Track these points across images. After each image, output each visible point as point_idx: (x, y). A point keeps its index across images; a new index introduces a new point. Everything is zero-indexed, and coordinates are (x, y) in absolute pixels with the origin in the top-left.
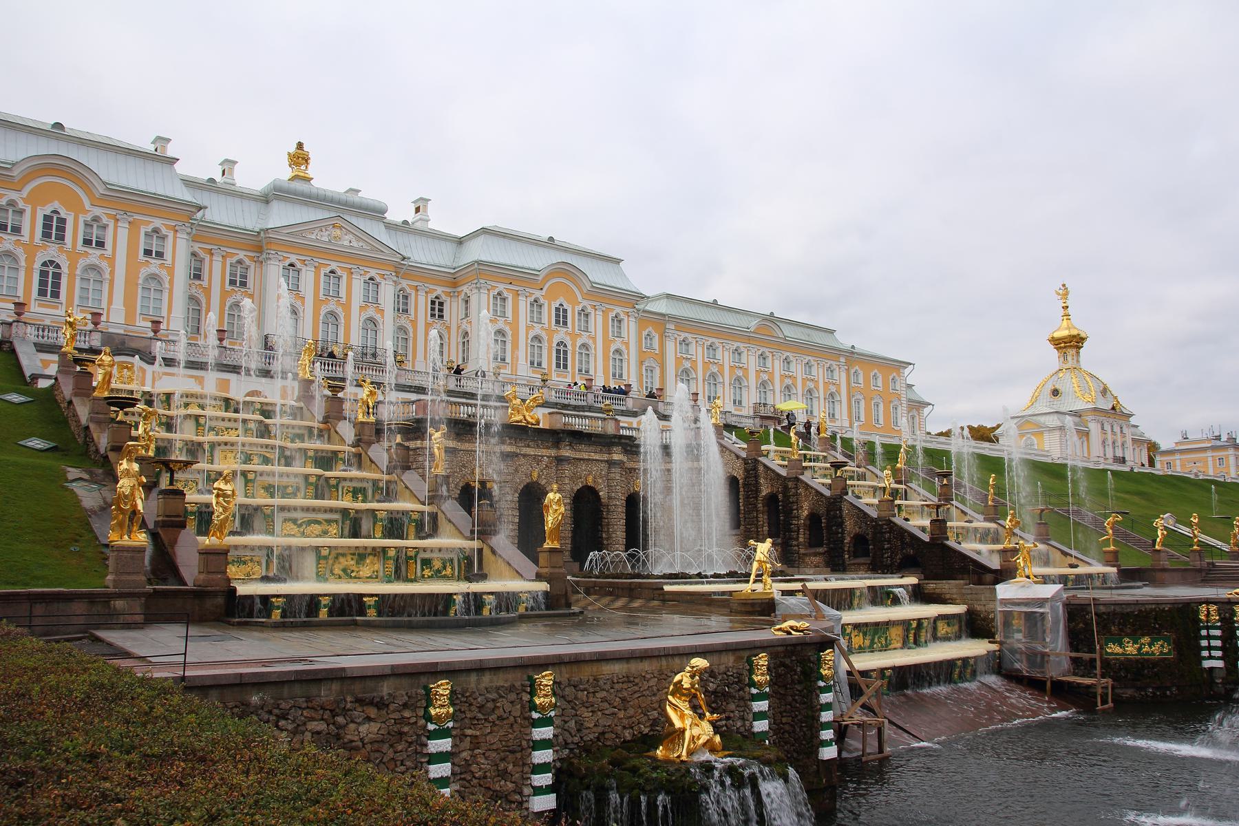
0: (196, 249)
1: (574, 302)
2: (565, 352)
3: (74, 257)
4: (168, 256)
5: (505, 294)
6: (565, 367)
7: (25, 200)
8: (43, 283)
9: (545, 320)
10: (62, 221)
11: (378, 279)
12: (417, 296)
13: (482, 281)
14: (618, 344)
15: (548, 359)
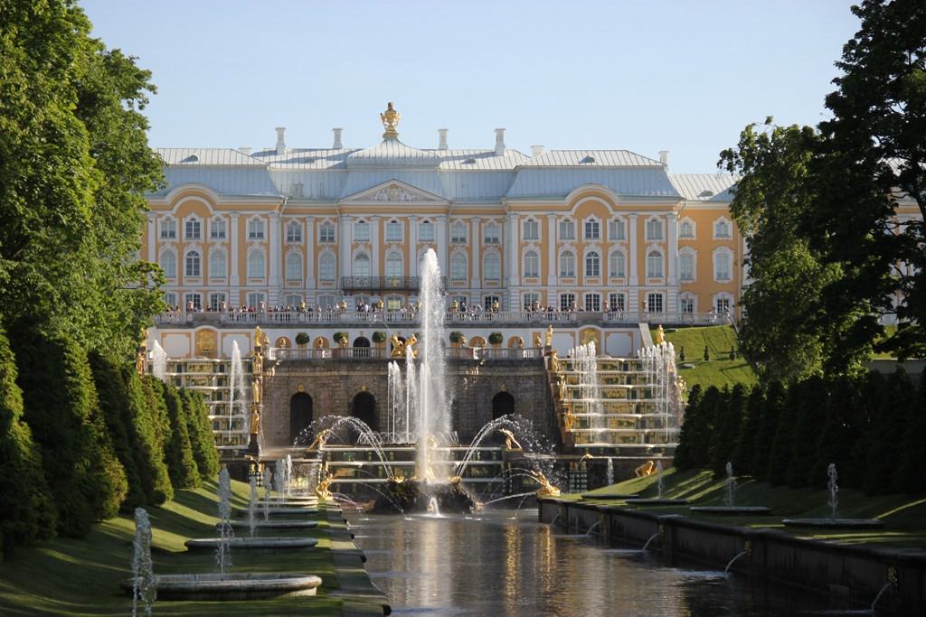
0: (294, 220)
1: (604, 214)
2: (596, 261)
3: (206, 247)
4: (265, 235)
5: (535, 220)
6: (597, 273)
7: (175, 216)
8: (189, 267)
9: (576, 237)
10: (198, 224)
11: (430, 220)
12: (471, 226)
13: (513, 212)
14: (655, 247)
15: (579, 267)
